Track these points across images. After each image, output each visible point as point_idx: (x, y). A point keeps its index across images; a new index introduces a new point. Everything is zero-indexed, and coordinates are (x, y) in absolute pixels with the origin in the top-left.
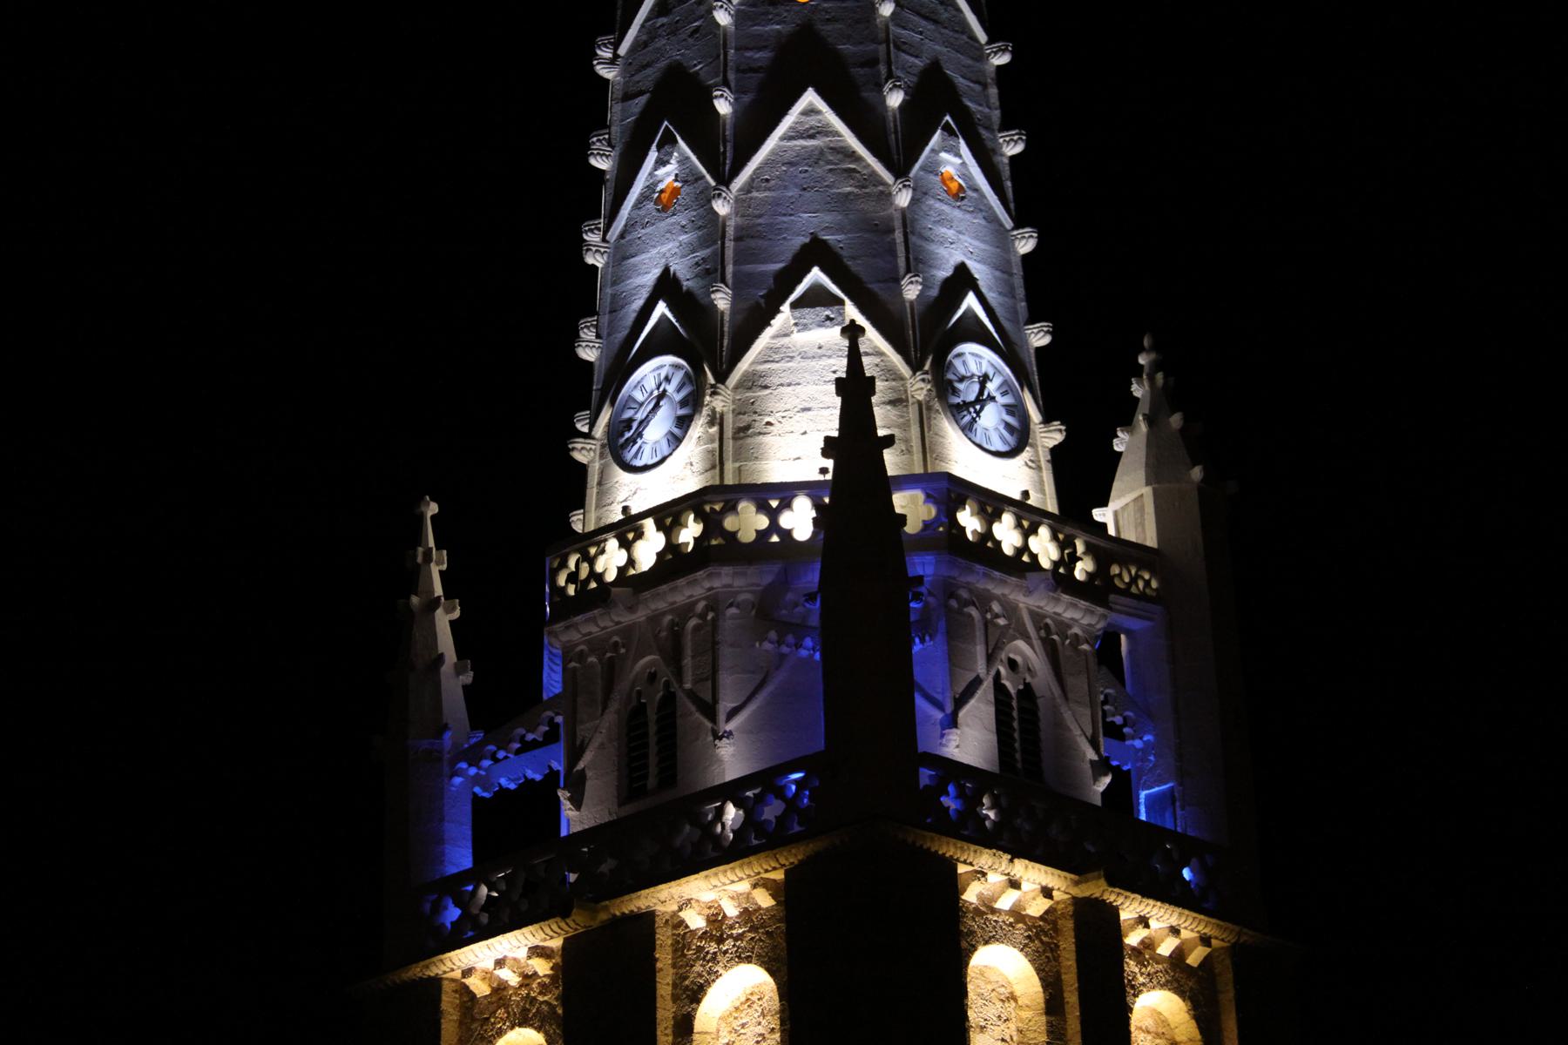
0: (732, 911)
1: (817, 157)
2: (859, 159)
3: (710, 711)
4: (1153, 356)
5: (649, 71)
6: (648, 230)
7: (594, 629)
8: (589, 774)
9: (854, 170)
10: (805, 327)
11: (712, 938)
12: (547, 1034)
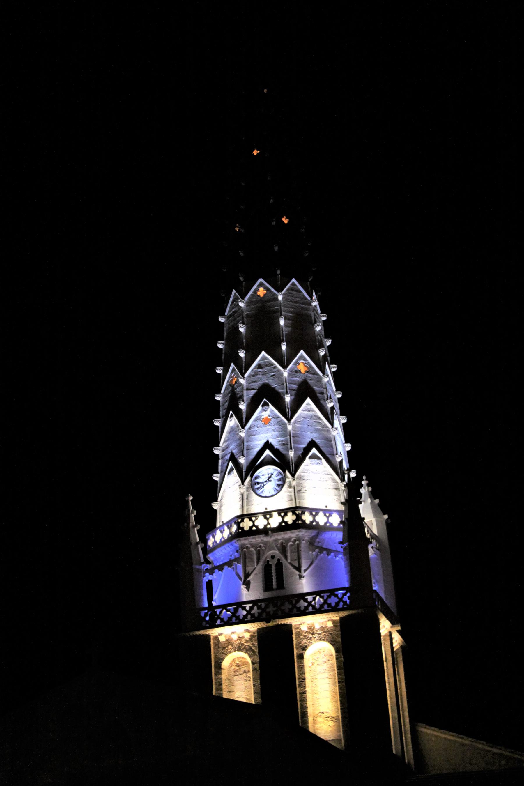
0: (317, 627)
1: (311, 417)
2: (321, 419)
3: (299, 569)
4: (367, 482)
5: (256, 383)
6: (260, 429)
7: (254, 541)
8: (251, 582)
9: (320, 422)
10: (313, 464)
11: (309, 633)
12: (248, 654)
